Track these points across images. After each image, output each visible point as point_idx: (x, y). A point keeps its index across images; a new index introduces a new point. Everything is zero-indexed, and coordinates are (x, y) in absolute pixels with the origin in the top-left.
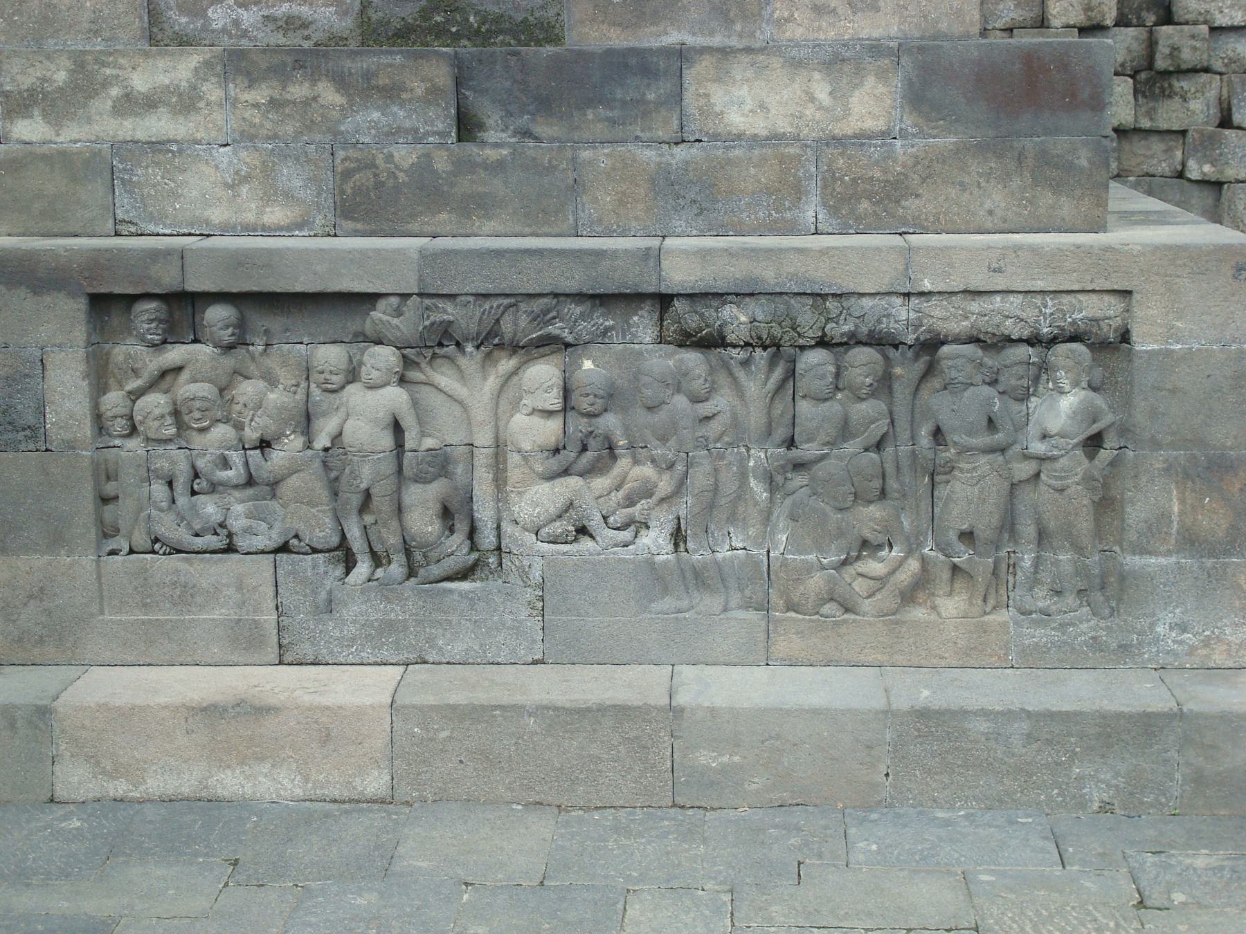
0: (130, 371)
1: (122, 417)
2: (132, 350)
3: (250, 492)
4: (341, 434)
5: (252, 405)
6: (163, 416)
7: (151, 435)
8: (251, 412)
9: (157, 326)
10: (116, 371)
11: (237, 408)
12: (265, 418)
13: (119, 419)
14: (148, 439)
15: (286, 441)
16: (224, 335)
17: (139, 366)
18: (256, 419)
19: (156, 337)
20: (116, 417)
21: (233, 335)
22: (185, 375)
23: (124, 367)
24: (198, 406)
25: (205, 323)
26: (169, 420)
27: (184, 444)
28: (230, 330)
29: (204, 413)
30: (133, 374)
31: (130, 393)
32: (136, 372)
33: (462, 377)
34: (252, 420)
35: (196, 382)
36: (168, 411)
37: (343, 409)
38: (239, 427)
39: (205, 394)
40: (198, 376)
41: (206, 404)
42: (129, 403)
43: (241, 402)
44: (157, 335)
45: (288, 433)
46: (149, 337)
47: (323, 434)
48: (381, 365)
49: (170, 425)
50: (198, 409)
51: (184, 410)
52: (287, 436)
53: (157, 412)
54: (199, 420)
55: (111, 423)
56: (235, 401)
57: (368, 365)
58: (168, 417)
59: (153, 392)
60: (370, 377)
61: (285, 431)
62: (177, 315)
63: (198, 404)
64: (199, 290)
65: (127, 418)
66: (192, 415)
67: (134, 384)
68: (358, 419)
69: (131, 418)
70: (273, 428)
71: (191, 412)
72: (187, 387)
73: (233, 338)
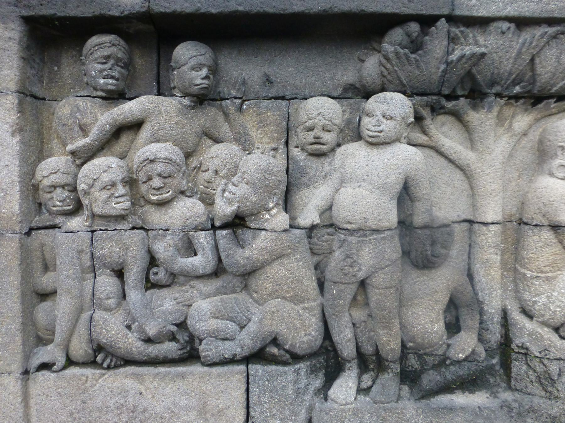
0: (77, 129)
1: (63, 187)
2: (81, 102)
3: (216, 283)
4: (330, 208)
5: (225, 171)
6: (113, 185)
7: (97, 210)
8: (223, 181)
9: (113, 65)
10: (59, 128)
11: (207, 176)
12: (243, 185)
13: (59, 190)
14: (94, 216)
15: (267, 216)
16: (196, 78)
17: (89, 120)
18: (230, 187)
19: (111, 81)
20: (55, 187)
21: (207, 77)
22: (145, 132)
23: (70, 122)
24: (159, 170)
25: (172, 64)
26: (121, 190)
27: (140, 223)
28: (204, 71)
29: (166, 181)
30: (80, 133)
31: (73, 153)
32: (84, 130)
33: (472, 142)
34: (224, 191)
35: (158, 141)
36: (121, 178)
37: (337, 175)
38: (208, 200)
39: (169, 156)
40: (160, 134)
41: (169, 169)
42: (73, 168)
43: (212, 168)
44: (112, 77)
45: (271, 206)
46: (102, 81)
47: (310, 207)
48: (396, 112)
49: (122, 196)
50: (160, 175)
51: (142, 176)
52: (268, 210)
53: (106, 178)
54: (158, 189)
55: (48, 196)
56: (203, 168)
57: (379, 113)
58: (120, 186)
59: (105, 156)
60: (380, 129)
61: (267, 203)
62: (140, 62)
63: (159, 167)
64: (168, 11)
65: (70, 188)
66: (151, 183)
67: (81, 142)
68: (360, 186)
69: (74, 190)
70: (254, 199)
71: (150, 179)
72: (147, 148)
73: (206, 82)
